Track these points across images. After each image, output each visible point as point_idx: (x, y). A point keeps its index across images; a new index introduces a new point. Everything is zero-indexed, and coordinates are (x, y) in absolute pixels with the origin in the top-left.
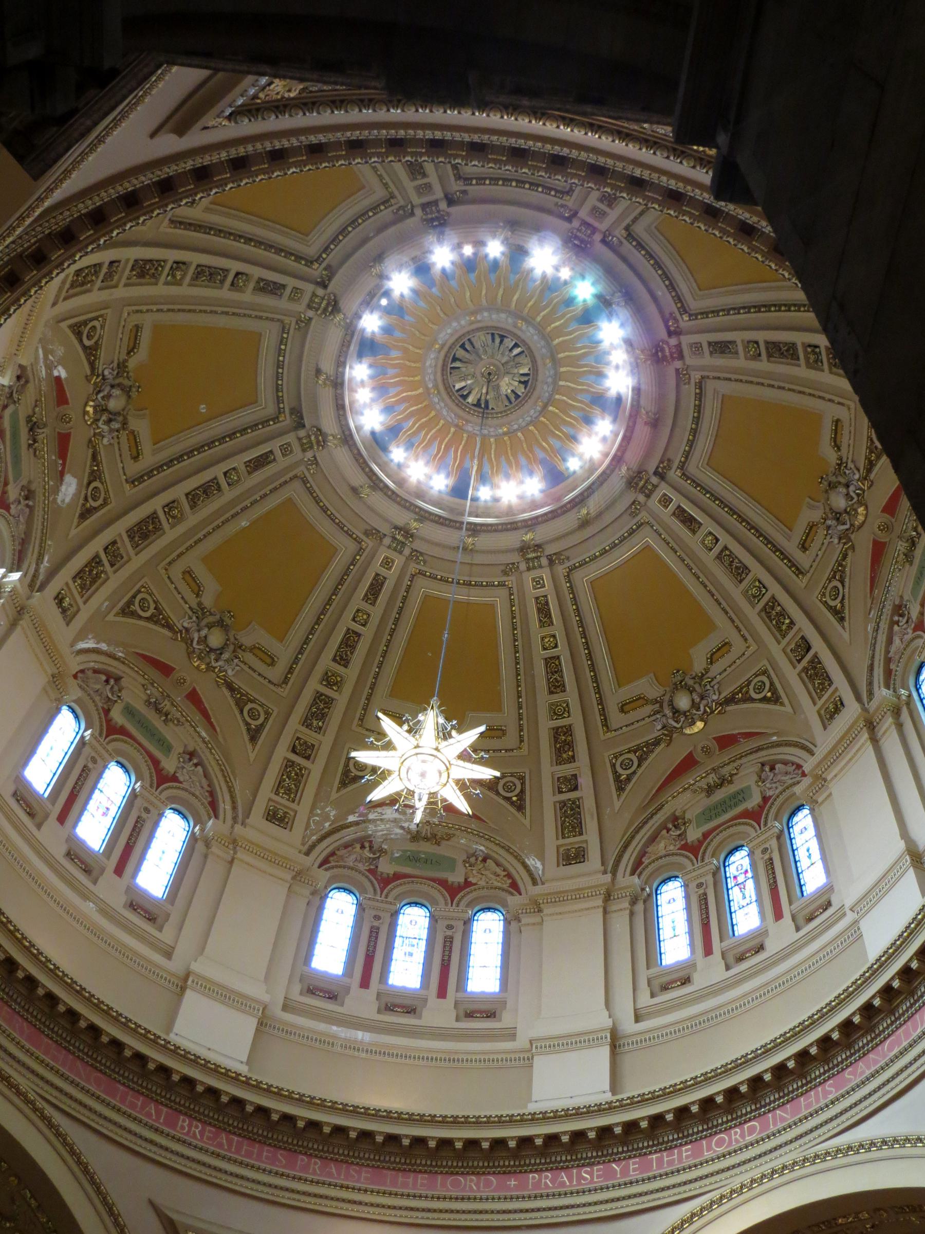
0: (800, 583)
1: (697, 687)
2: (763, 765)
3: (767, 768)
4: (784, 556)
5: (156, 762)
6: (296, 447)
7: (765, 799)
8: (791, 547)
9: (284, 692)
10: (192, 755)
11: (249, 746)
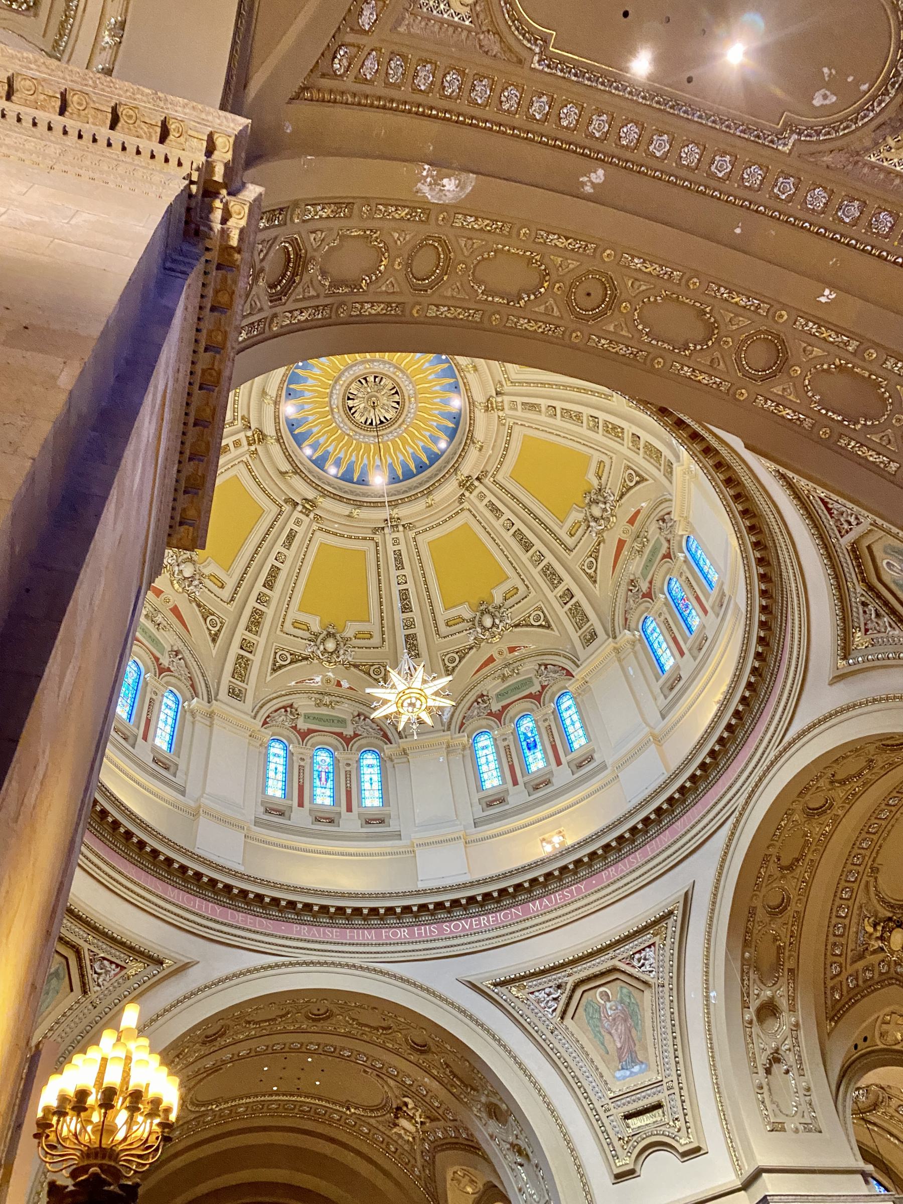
0: (568, 557)
1: (497, 613)
2: (540, 665)
3: (543, 668)
4: (557, 538)
5: (157, 659)
6: (244, 442)
7: (543, 687)
8: (563, 534)
9: (231, 608)
10: (177, 653)
11: (212, 645)
